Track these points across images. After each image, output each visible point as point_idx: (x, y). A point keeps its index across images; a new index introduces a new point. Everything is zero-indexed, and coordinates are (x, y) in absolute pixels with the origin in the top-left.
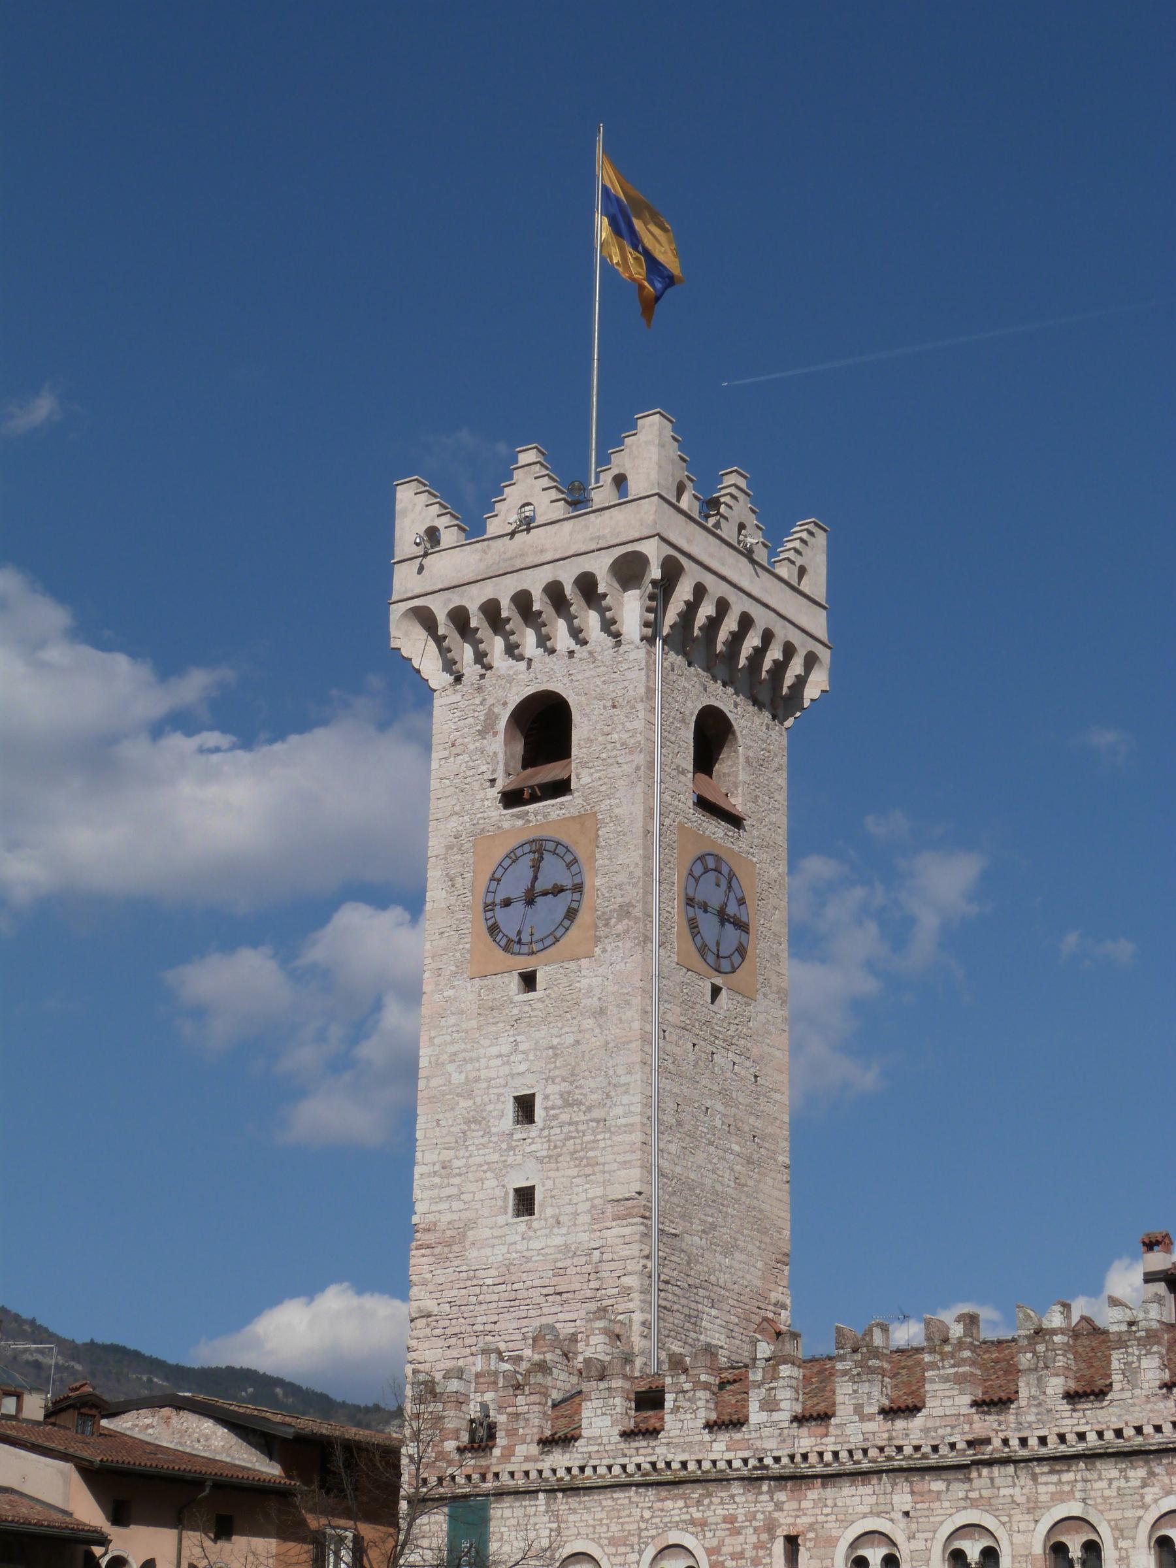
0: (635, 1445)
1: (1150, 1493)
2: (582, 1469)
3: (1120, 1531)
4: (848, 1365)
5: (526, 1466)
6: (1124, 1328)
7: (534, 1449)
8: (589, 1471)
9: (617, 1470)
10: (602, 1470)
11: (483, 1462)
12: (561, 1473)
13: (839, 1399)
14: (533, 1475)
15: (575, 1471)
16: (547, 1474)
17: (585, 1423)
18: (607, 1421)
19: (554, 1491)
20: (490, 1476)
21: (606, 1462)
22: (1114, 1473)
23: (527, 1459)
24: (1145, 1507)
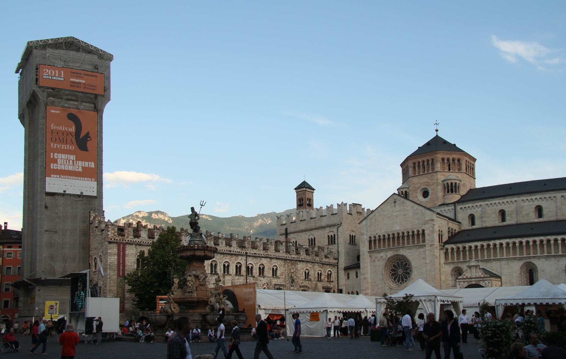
0: (150, 239)
1: (224, 259)
2: (141, 242)
3: (220, 263)
4: (184, 234)
5: (131, 240)
6: (221, 237)
7: (132, 237)
8: (142, 242)
9: (147, 243)
10: (145, 243)
11: (123, 238)
12: (137, 242)
13: (183, 239)
14: (132, 241)
15: (140, 242)
16: (135, 241)
17: (141, 235)
18: (145, 235)
19: (136, 244)
20: (124, 240)
21: (146, 241)
22: (219, 255)
23: (131, 239)
24: (223, 260)
